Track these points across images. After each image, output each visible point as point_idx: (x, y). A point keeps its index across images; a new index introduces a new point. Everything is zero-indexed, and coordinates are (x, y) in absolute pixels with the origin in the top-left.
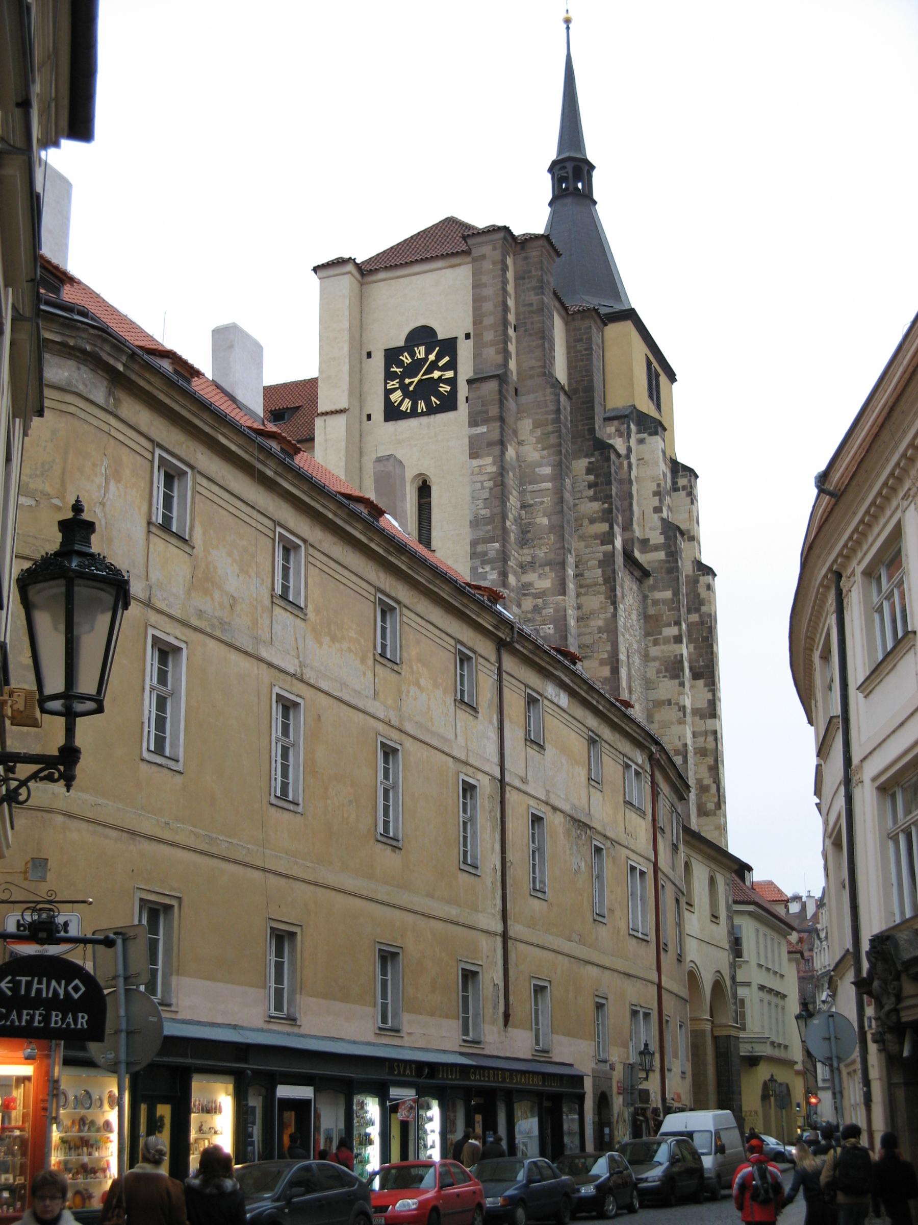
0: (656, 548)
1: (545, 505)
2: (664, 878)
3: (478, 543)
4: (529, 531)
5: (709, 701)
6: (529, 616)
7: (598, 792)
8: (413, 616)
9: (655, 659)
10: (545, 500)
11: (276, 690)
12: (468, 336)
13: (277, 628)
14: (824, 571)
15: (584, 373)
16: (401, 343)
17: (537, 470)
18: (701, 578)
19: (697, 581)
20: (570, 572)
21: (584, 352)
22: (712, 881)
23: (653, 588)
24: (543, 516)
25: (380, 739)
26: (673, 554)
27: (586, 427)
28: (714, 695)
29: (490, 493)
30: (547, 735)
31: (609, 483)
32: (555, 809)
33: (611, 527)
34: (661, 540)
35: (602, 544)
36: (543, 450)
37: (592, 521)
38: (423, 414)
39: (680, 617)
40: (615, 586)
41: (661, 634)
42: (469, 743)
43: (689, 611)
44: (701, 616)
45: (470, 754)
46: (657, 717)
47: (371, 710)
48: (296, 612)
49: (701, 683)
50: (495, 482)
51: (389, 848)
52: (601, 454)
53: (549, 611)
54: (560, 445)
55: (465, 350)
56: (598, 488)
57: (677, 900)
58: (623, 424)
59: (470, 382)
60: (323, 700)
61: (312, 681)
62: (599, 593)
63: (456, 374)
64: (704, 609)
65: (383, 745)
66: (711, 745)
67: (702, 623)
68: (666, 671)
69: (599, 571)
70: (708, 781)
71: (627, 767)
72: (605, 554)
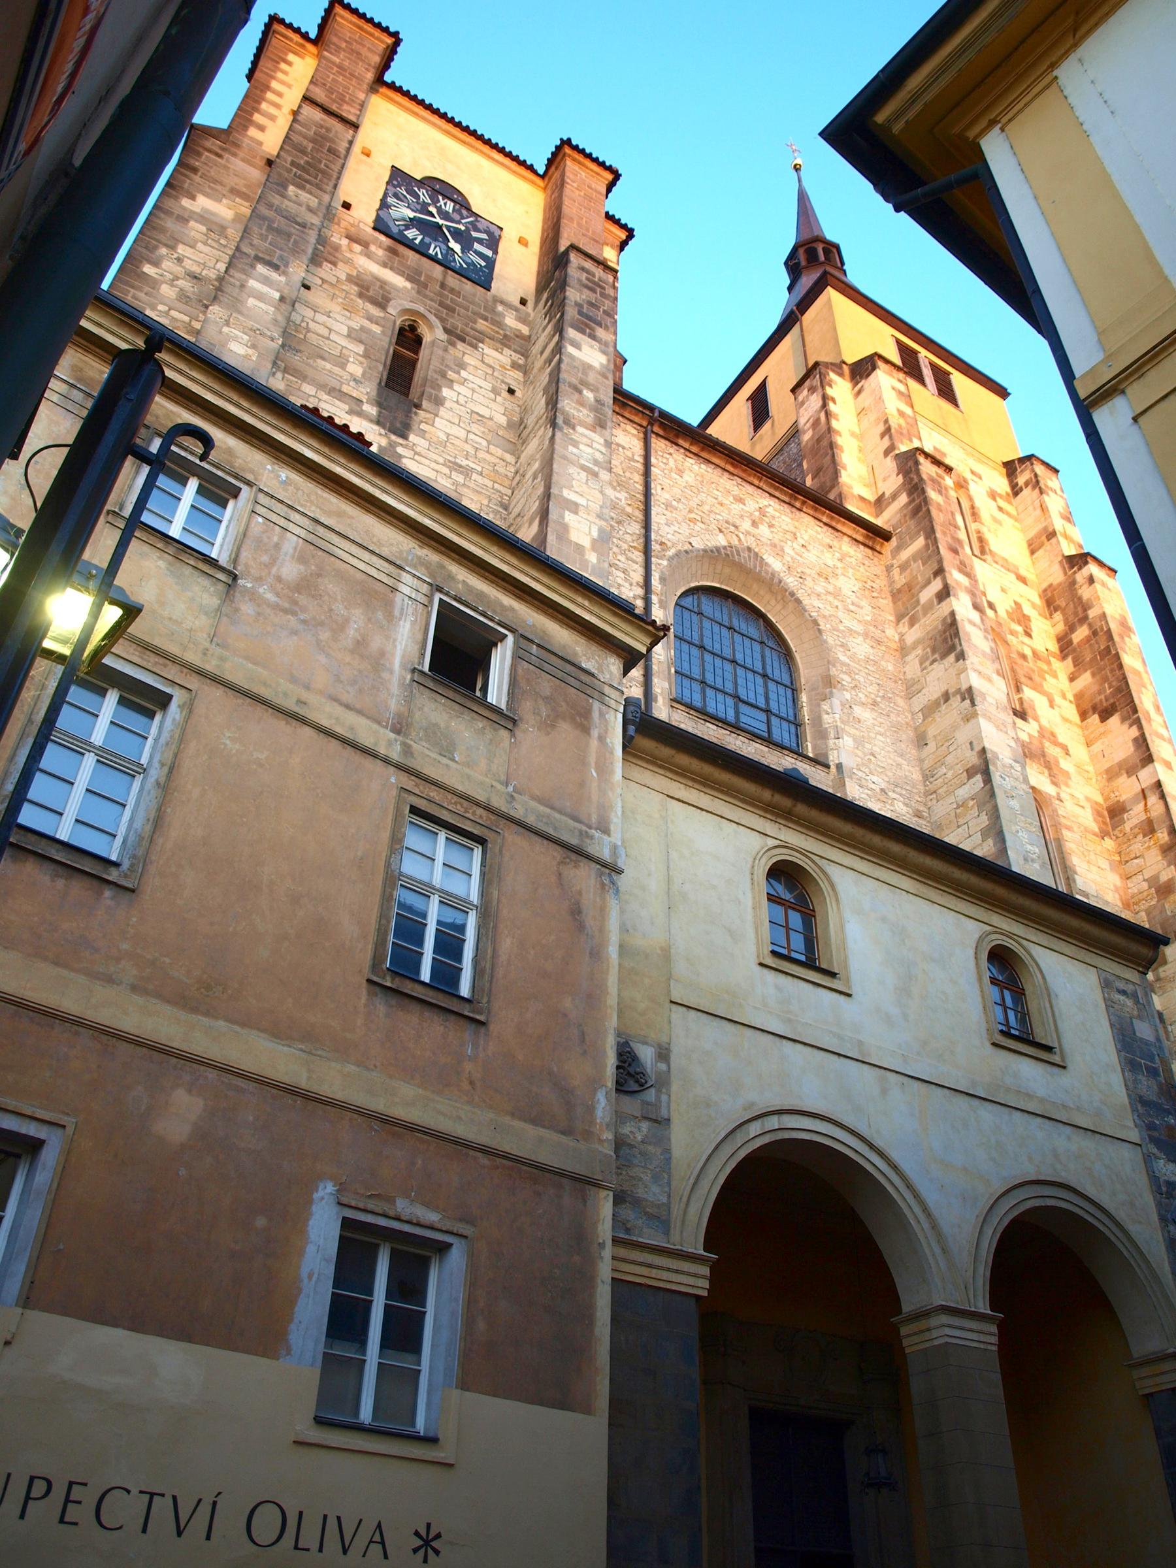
0: (894, 496)
5: (1135, 740)
18: (1081, 576)
19: (1074, 583)
28: (1140, 728)
41: (918, 601)
44: (1090, 626)
46: (932, 732)
49: (1115, 720)
64: (1092, 613)
68: (934, 651)
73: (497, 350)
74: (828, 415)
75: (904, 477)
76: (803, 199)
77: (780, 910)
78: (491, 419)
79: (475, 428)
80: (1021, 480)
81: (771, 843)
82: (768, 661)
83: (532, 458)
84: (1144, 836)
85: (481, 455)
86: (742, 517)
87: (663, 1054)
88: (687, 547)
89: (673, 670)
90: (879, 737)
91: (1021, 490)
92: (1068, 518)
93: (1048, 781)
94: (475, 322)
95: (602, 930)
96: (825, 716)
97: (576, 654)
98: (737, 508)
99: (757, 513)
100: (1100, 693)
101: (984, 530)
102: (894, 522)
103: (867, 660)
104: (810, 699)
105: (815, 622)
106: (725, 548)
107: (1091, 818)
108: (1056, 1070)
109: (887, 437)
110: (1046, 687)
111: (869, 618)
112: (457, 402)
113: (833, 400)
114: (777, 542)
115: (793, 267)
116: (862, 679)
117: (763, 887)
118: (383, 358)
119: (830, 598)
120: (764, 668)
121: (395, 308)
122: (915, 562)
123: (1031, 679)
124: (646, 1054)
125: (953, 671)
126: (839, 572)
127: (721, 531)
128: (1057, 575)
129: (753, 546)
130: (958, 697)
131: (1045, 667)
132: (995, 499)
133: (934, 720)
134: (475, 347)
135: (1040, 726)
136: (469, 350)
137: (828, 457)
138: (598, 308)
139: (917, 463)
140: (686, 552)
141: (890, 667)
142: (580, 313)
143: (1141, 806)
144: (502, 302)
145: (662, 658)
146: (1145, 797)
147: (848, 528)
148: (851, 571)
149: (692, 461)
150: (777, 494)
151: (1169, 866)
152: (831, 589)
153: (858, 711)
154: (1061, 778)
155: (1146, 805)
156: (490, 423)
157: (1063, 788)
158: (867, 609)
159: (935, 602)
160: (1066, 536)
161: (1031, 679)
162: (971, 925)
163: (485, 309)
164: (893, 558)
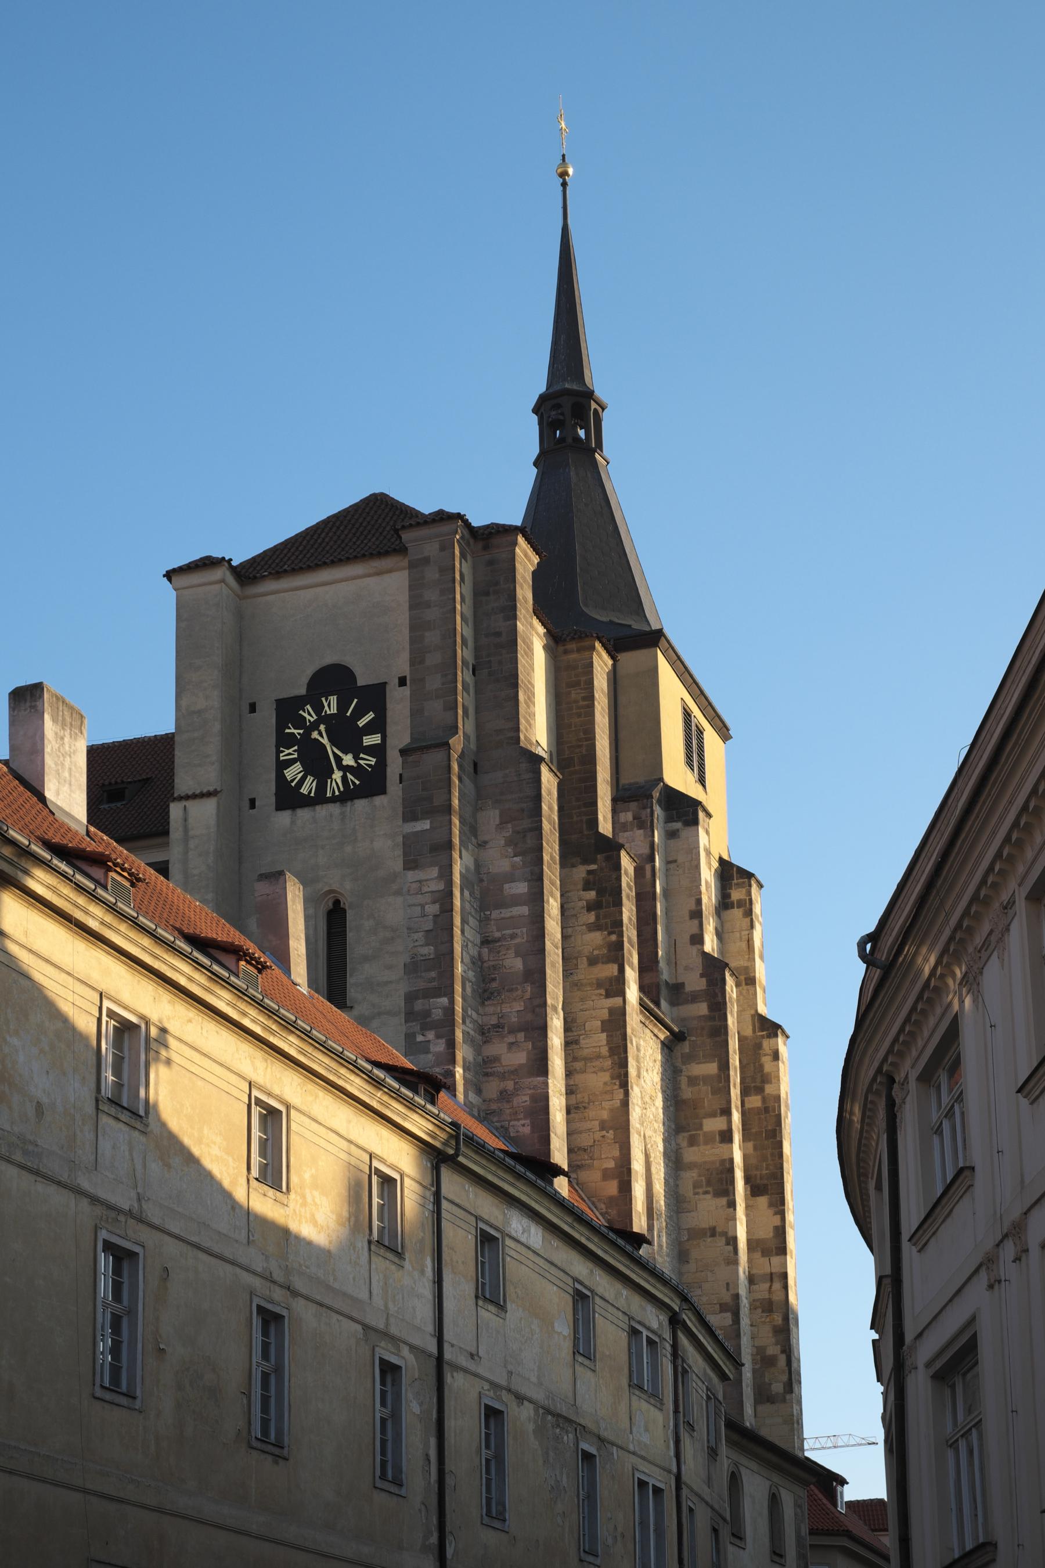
0: (694, 998)
1: (517, 941)
2: (695, 1499)
3: (417, 998)
4: (494, 979)
5: (776, 1228)
6: (494, 1106)
7: (589, 1373)
8: (307, 1121)
9: (692, 1166)
10: (518, 931)
11: (103, 1234)
12: (402, 682)
13: (105, 1145)
14: (871, 1073)
15: (582, 735)
16: (303, 691)
17: (506, 886)
19: (759, 1046)
20: (556, 1040)
21: (582, 703)
22: (774, 1500)
23: (689, 1058)
24: (517, 955)
25: (256, 1301)
26: (718, 1007)
27: (584, 818)
28: (783, 1219)
29: (435, 922)
30: (510, 1290)
31: (619, 904)
32: (520, 1398)
33: (622, 971)
34: (701, 984)
35: (608, 995)
36: (515, 856)
37: (593, 961)
38: (334, 799)
39: (729, 1102)
40: (626, 1058)
41: (700, 1127)
42: (391, 1305)
43: (745, 1092)
44: (764, 1100)
45: (392, 1320)
46: (694, 1254)
47: (243, 1260)
48: (133, 1122)
49: (763, 1201)
50: (442, 905)
51: (270, 1458)
52: (608, 859)
53: (523, 1100)
54: (540, 849)
55: (399, 705)
56: (602, 912)
57: (715, 1531)
58: (644, 808)
59: (404, 752)
60: (172, 1247)
61: (156, 1221)
62: (602, 1070)
63: (384, 738)
64: (769, 1089)
65: (260, 1308)
66: (777, 1297)
67: (766, 1110)
68: (709, 1183)
69: (604, 1035)
70: (773, 1350)
71: (634, 1333)
72: (611, 1011)
84: (763, 1312)
122: (705, 1084)
130: (724, 1239)
143: (768, 1285)
146: (772, 1280)
151: (776, 1344)
164: (684, 1063)
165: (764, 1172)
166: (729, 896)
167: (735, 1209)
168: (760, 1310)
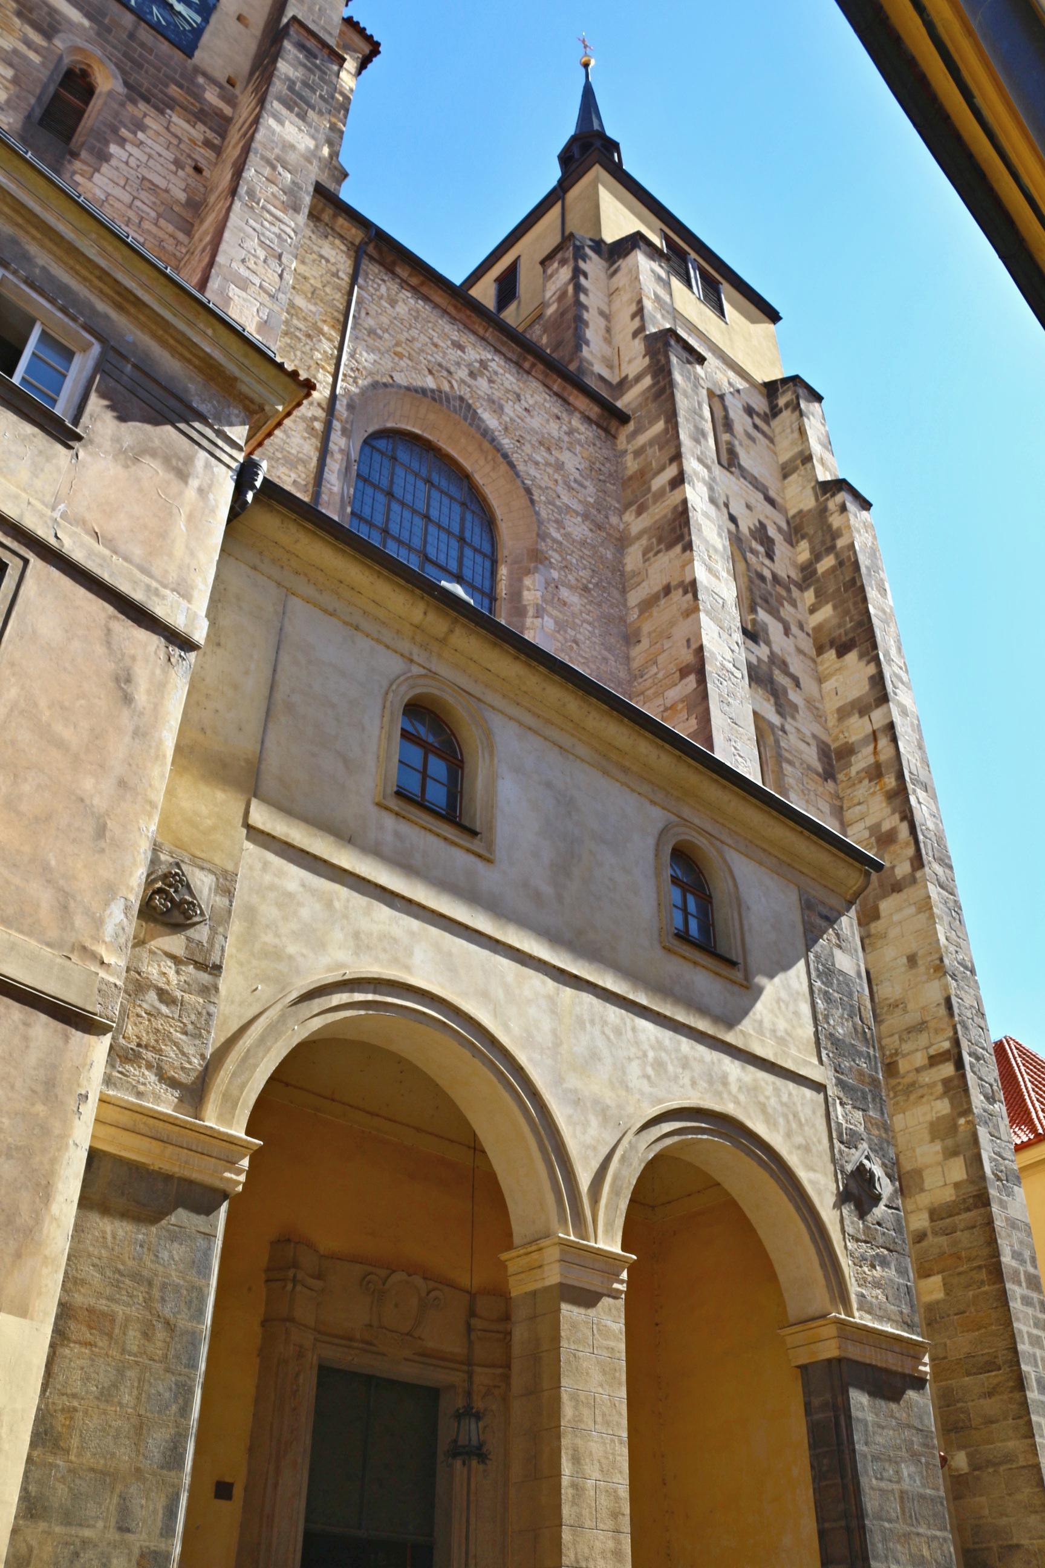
0: (638, 379)
5: (872, 678)
41: (649, 489)
44: (837, 556)
49: (852, 657)
64: (840, 543)
68: (660, 541)
73: (188, 122)
74: (579, 288)
75: (651, 358)
76: (588, 94)
77: (416, 755)
78: (167, 191)
79: (143, 195)
80: (782, 402)
81: (416, 670)
82: (468, 524)
83: (206, 233)
84: (870, 781)
85: (146, 225)
86: (458, 364)
87: (226, 885)
88: (386, 379)
89: (349, 510)
90: (585, 625)
91: (781, 411)
92: (828, 445)
93: (773, 709)
94: (167, 86)
95: (156, 708)
96: (525, 593)
97: (186, 390)
98: (454, 354)
99: (477, 365)
100: (840, 626)
101: (736, 443)
102: (633, 406)
103: (583, 543)
104: (511, 573)
105: (528, 491)
106: (433, 391)
107: (815, 757)
108: (736, 989)
109: (638, 319)
110: (782, 613)
111: (592, 500)
112: (127, 163)
113: (586, 276)
114: (495, 398)
115: (566, 158)
116: (574, 561)
117: (399, 723)
118: (38, 91)
119: (550, 470)
120: (462, 529)
121: (63, 41)
123: (767, 601)
124: (202, 883)
125: (678, 563)
126: (565, 446)
127: (430, 372)
128: (807, 502)
129: (467, 396)
130: (680, 591)
131: (784, 593)
132: (751, 416)
133: (651, 616)
134: (162, 113)
135: (771, 652)
136: (152, 112)
137: (571, 331)
138: (314, 91)
139: (667, 344)
140: (385, 385)
141: (609, 555)
142: (291, 88)
143: (871, 748)
144: (205, 75)
145: (336, 489)
146: (875, 740)
147: (581, 402)
148: (578, 447)
149: (409, 295)
150: (504, 350)
151: (893, 813)
152: (552, 460)
153: (564, 593)
154: (787, 709)
155: (875, 748)
156: (165, 195)
157: (789, 719)
158: (591, 489)
159: (668, 489)
160: (823, 464)
161: (767, 601)
162: (656, 813)
163: (182, 75)
164: (628, 442)
165: (849, 625)
166: (777, 405)
167: (691, 550)
168: (866, 781)
